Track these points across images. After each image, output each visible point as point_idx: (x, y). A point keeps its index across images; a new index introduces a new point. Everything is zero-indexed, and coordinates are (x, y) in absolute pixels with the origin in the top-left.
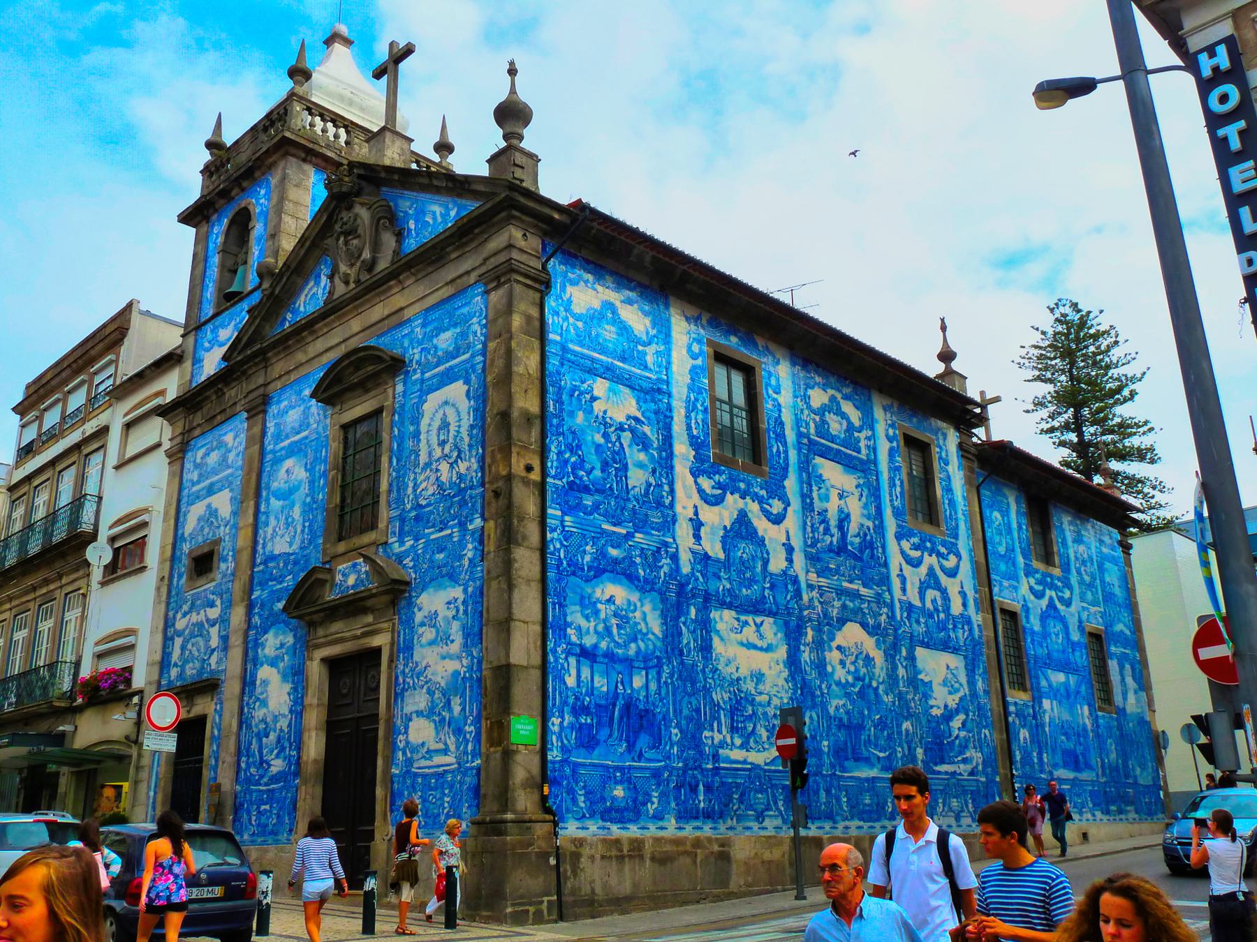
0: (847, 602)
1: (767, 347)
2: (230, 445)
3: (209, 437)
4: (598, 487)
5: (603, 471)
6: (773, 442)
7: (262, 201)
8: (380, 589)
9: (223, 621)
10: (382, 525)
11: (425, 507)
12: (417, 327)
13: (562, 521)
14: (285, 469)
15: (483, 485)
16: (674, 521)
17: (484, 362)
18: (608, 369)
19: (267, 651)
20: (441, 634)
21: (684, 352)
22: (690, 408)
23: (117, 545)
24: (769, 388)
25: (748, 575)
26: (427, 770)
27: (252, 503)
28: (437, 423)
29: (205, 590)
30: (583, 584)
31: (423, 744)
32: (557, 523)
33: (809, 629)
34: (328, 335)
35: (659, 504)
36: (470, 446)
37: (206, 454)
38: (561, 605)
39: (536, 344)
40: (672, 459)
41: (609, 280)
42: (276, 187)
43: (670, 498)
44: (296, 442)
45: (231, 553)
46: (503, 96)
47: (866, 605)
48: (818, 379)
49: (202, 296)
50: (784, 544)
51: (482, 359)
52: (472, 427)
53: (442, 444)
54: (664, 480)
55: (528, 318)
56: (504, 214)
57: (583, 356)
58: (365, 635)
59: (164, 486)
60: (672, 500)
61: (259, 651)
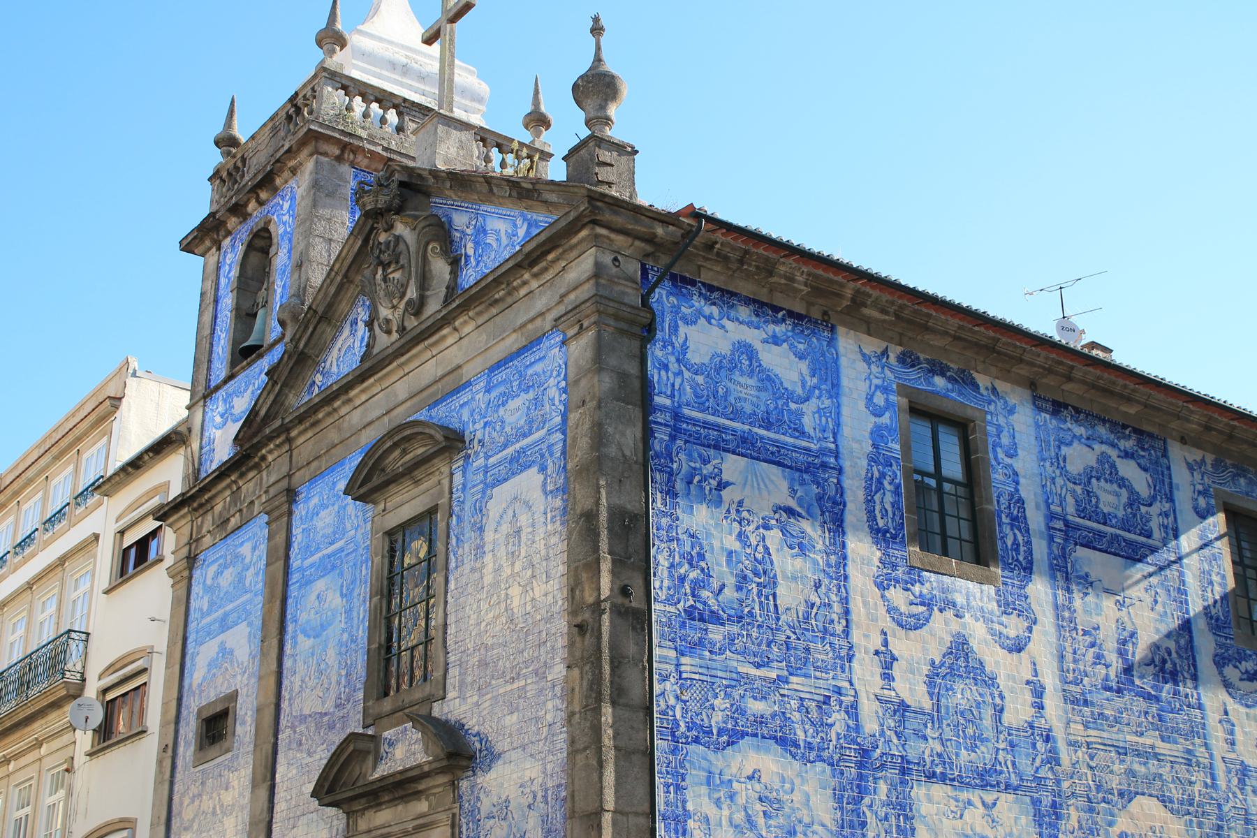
0: (1136, 767)
1: (994, 389)
2: (247, 560)
3: (221, 550)
4: (732, 612)
5: (739, 589)
6: (1007, 529)
7: (285, 218)
8: (434, 766)
10: (437, 674)
11: (493, 647)
12: (478, 391)
13: (678, 665)
14: (313, 597)
16: (850, 659)
17: (565, 441)
18: (744, 440)
20: (514, 830)
21: (862, 405)
22: (873, 487)
23: (110, 696)
24: (999, 450)
25: (970, 731)
27: (275, 642)
28: (505, 528)
29: (219, 764)
30: (711, 755)
32: (671, 668)
33: (1072, 810)
34: (367, 404)
35: (825, 631)
37: (219, 573)
38: (678, 788)
39: (637, 413)
40: (845, 565)
41: (744, 312)
42: (303, 198)
43: (844, 623)
44: (329, 556)
45: (249, 713)
46: (584, 66)
47: (1168, 769)
48: (1080, 431)
49: (211, 352)
50: (1028, 683)
52: (548, 535)
54: (834, 598)
55: (623, 377)
56: (584, 233)
57: (706, 425)
59: (166, 615)
60: (847, 626)
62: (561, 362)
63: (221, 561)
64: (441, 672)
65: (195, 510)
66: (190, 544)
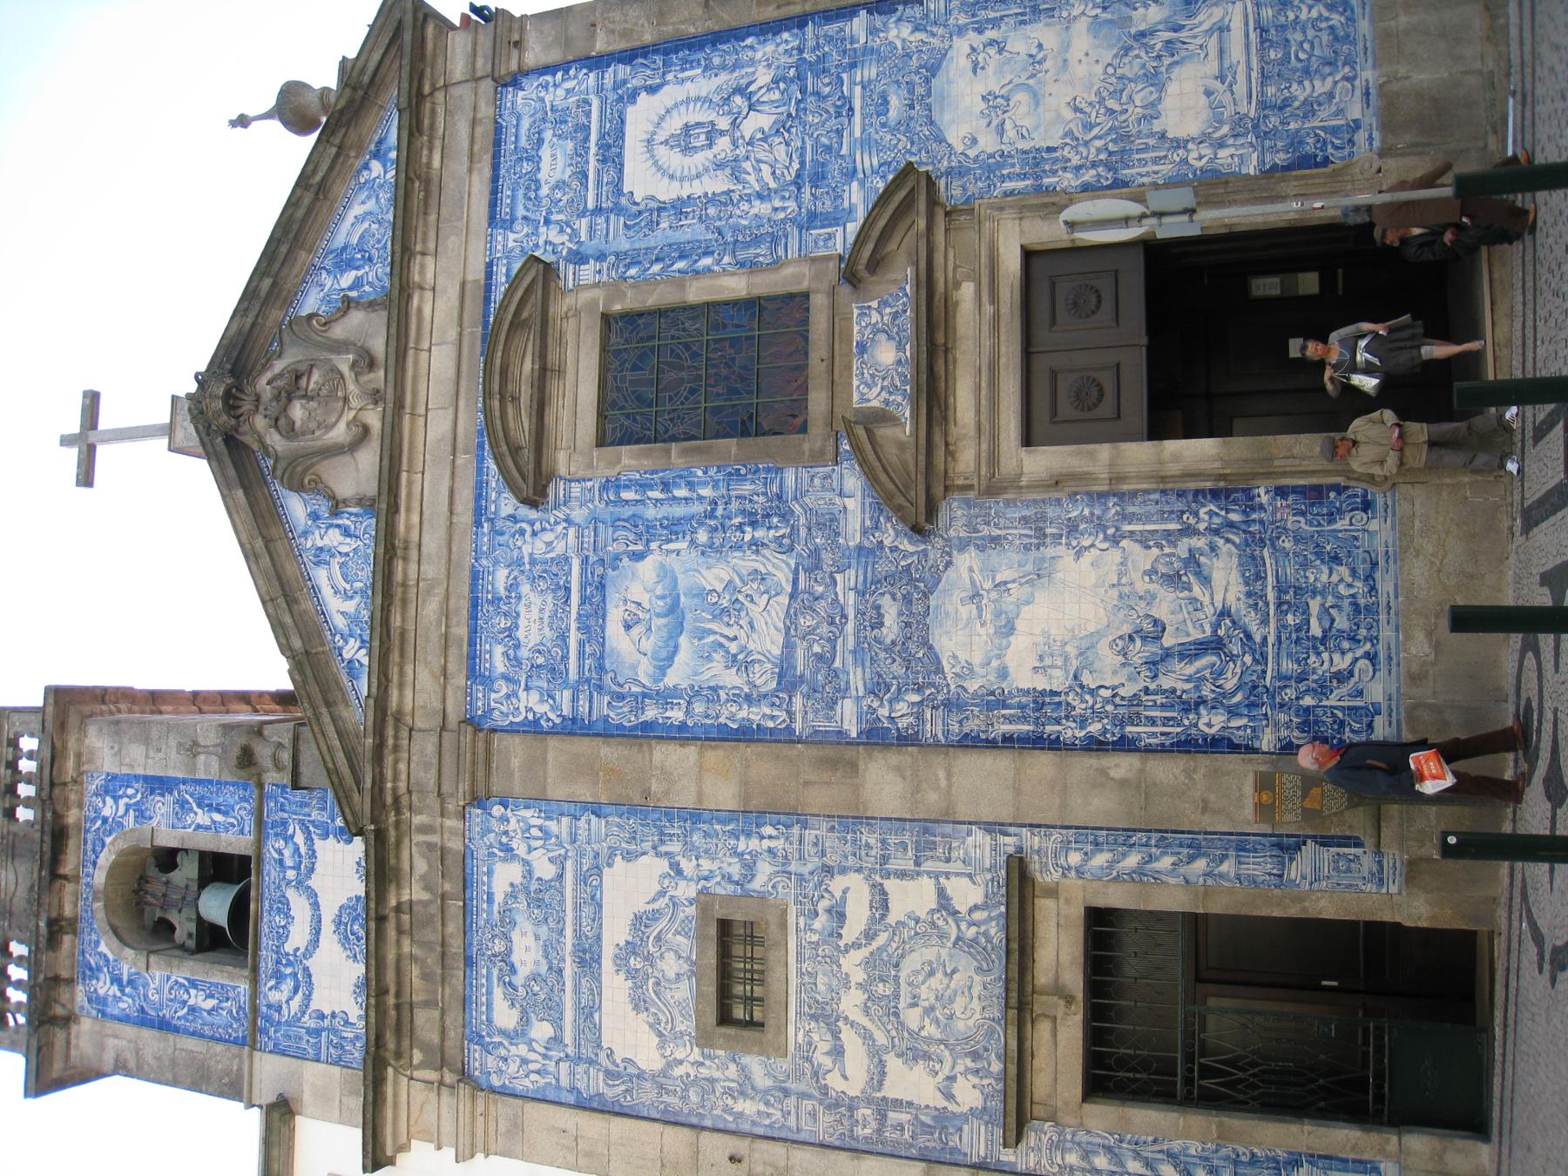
7: (121, 812)
9: (885, 859)
15: (800, 22)
19: (977, 660)
26: (1254, 75)
28: (673, 159)
31: (1208, 93)
34: (425, 517)
36: (736, 66)
44: (584, 600)
51: (611, 70)
52: (706, 69)
53: (712, 133)
58: (994, 298)
61: (973, 686)
62: (536, 84)
63: (495, 972)
64: (805, 269)
65: (398, 1055)
66: (441, 1083)
